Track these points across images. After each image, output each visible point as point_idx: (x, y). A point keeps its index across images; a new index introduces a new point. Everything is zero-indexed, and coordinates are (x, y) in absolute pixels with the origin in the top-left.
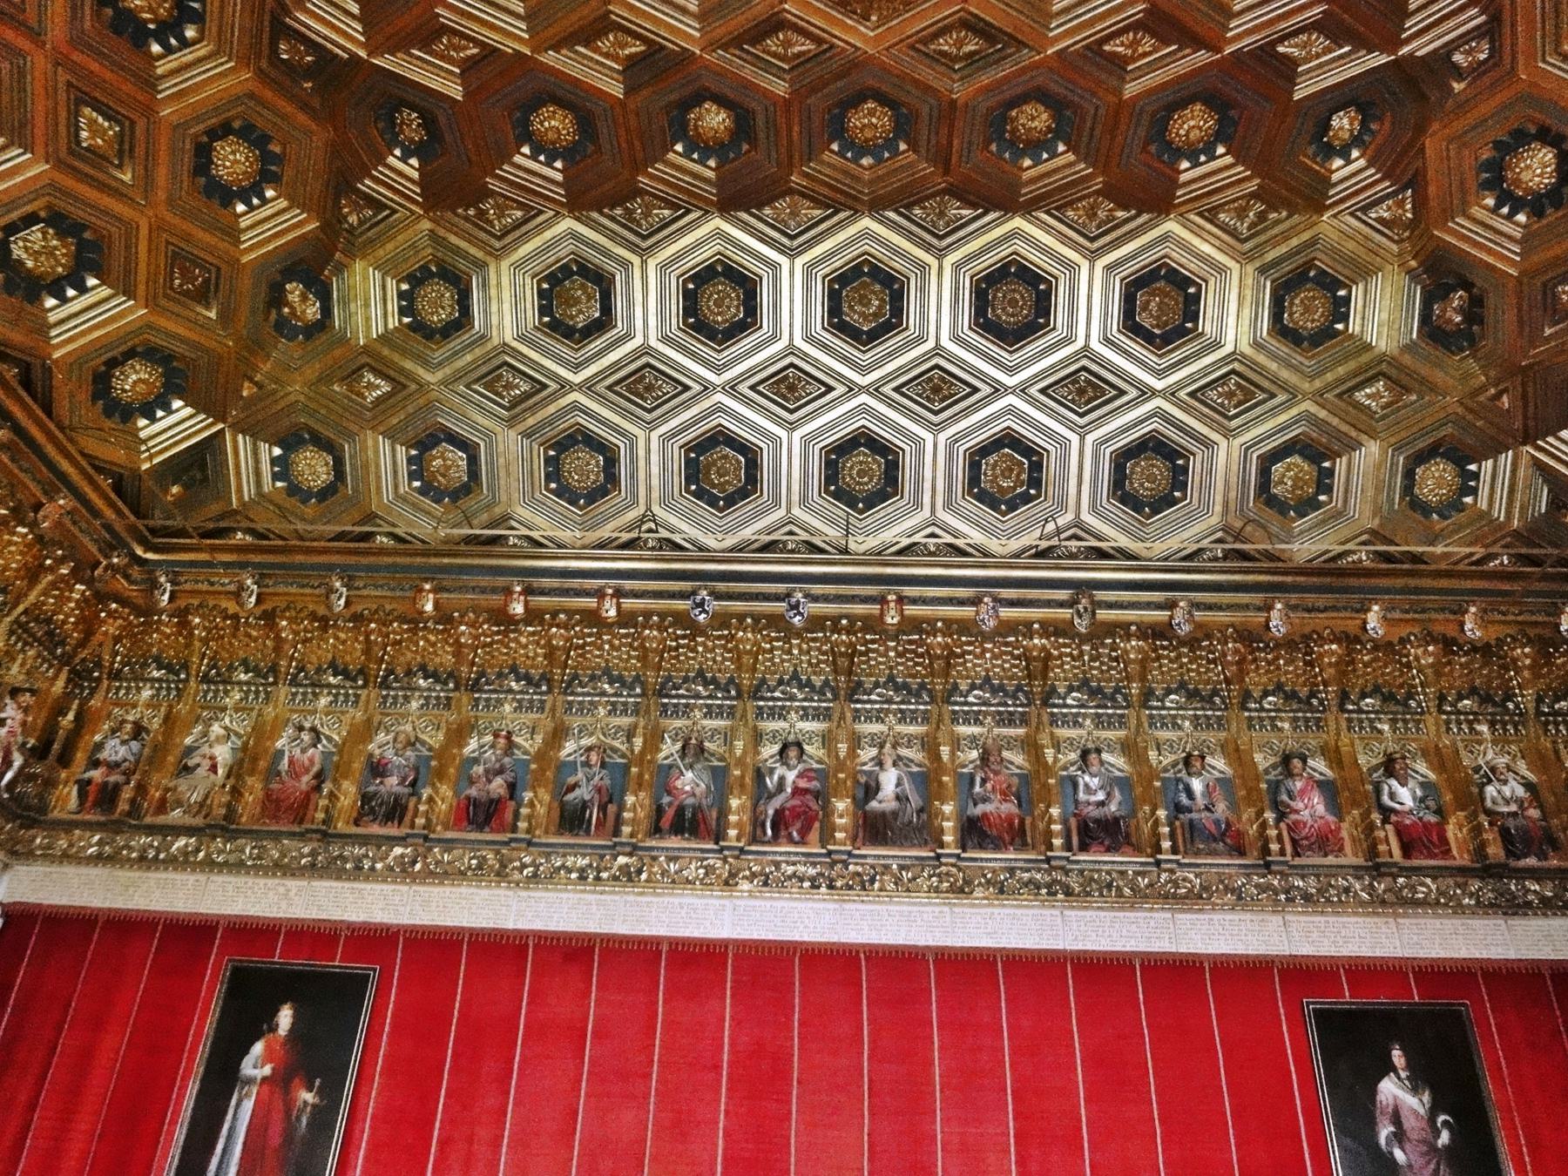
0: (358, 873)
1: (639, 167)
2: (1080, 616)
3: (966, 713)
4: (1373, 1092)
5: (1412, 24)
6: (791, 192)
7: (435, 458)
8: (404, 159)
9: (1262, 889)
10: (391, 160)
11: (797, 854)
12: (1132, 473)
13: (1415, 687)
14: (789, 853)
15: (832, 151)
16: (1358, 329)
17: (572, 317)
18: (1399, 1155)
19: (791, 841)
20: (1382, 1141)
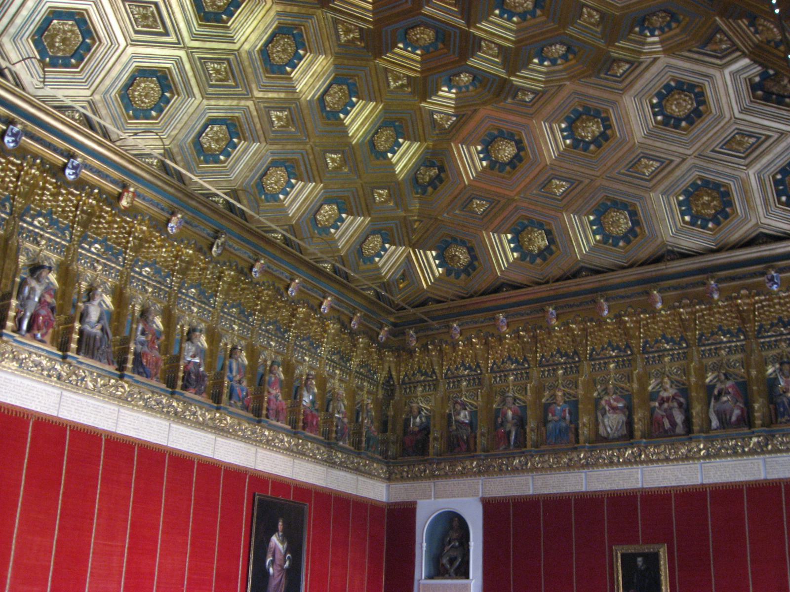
2: (218, 247)
3: (30, 231)
4: (269, 540)
5: (524, 73)
9: (37, 364)
11: (43, 350)
13: (323, 342)
14: (39, 348)
16: (348, 123)
18: (271, 570)
19: (34, 337)
20: (267, 564)
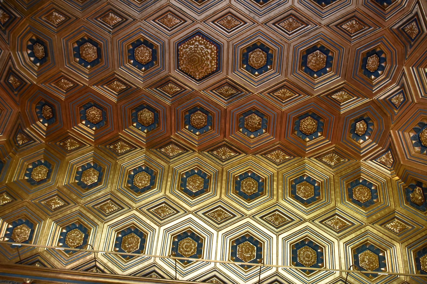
1: (120, 129)
6: (171, 143)
7: (18, 229)
8: (43, 123)
10: (38, 123)
12: (299, 254)
15: (186, 129)
17: (86, 181)
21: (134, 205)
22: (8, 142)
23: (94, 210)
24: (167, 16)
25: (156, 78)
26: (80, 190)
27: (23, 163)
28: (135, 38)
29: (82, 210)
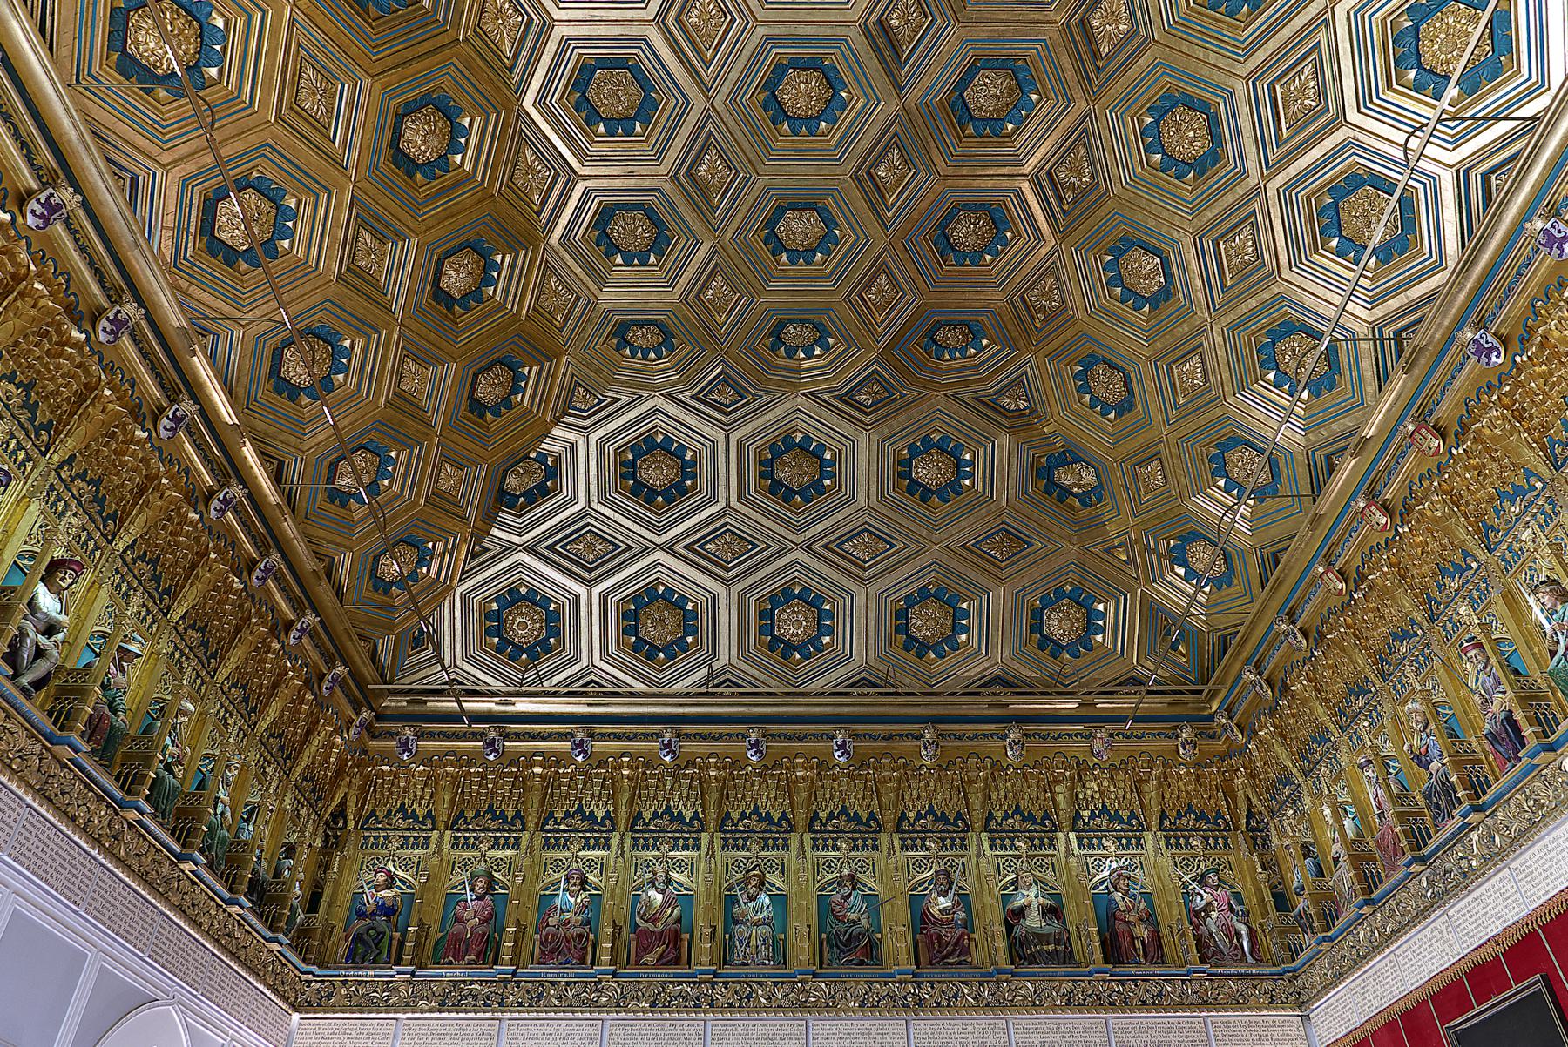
0: (1468, 879)
21: (1252, 182)
22: (1013, 430)
23: (1235, 290)
24: (693, 25)
25: (872, 63)
26: (1168, 309)
27: (1073, 412)
28: (758, 114)
29: (1225, 321)
